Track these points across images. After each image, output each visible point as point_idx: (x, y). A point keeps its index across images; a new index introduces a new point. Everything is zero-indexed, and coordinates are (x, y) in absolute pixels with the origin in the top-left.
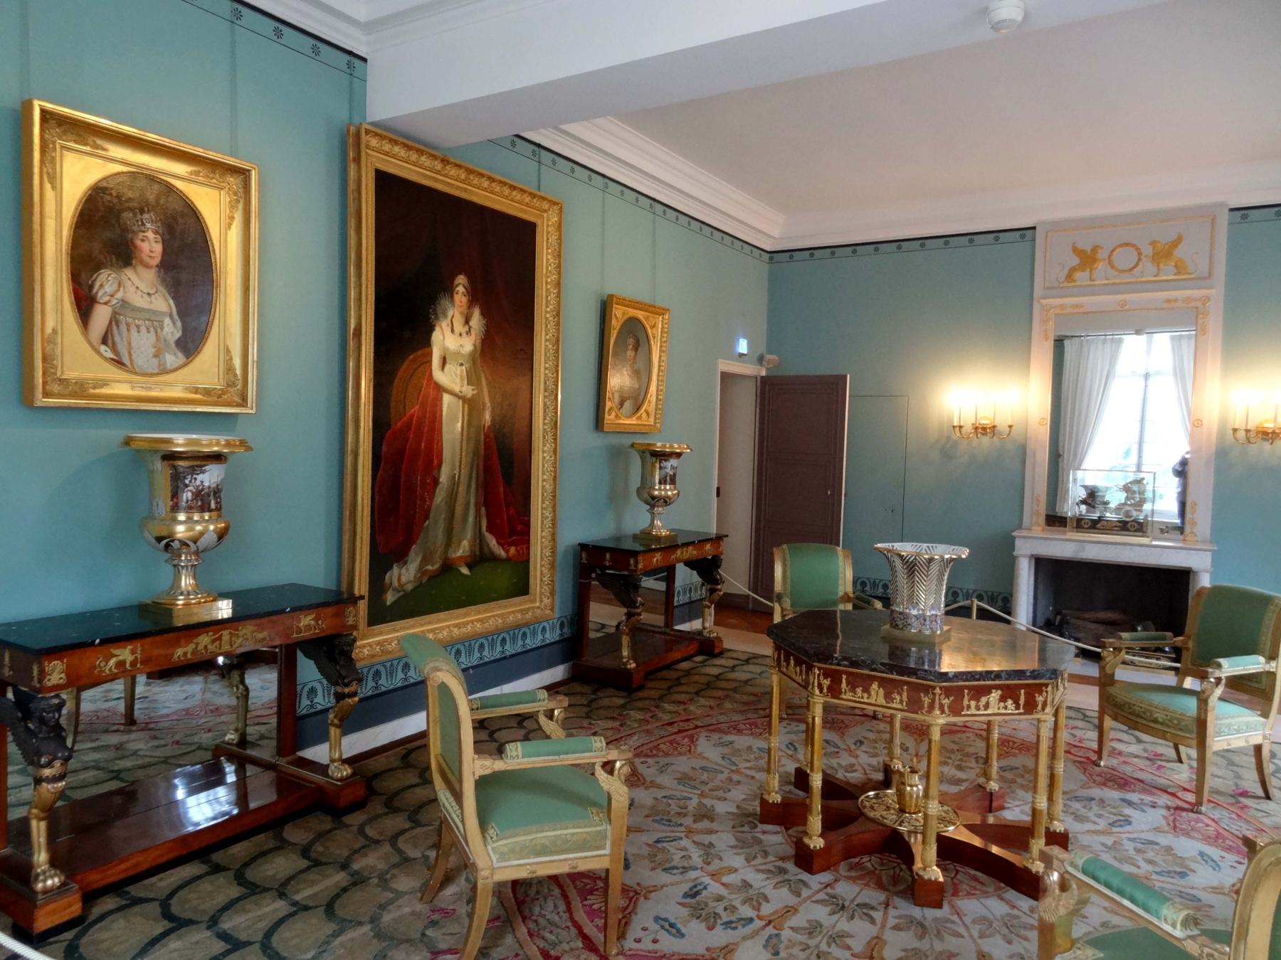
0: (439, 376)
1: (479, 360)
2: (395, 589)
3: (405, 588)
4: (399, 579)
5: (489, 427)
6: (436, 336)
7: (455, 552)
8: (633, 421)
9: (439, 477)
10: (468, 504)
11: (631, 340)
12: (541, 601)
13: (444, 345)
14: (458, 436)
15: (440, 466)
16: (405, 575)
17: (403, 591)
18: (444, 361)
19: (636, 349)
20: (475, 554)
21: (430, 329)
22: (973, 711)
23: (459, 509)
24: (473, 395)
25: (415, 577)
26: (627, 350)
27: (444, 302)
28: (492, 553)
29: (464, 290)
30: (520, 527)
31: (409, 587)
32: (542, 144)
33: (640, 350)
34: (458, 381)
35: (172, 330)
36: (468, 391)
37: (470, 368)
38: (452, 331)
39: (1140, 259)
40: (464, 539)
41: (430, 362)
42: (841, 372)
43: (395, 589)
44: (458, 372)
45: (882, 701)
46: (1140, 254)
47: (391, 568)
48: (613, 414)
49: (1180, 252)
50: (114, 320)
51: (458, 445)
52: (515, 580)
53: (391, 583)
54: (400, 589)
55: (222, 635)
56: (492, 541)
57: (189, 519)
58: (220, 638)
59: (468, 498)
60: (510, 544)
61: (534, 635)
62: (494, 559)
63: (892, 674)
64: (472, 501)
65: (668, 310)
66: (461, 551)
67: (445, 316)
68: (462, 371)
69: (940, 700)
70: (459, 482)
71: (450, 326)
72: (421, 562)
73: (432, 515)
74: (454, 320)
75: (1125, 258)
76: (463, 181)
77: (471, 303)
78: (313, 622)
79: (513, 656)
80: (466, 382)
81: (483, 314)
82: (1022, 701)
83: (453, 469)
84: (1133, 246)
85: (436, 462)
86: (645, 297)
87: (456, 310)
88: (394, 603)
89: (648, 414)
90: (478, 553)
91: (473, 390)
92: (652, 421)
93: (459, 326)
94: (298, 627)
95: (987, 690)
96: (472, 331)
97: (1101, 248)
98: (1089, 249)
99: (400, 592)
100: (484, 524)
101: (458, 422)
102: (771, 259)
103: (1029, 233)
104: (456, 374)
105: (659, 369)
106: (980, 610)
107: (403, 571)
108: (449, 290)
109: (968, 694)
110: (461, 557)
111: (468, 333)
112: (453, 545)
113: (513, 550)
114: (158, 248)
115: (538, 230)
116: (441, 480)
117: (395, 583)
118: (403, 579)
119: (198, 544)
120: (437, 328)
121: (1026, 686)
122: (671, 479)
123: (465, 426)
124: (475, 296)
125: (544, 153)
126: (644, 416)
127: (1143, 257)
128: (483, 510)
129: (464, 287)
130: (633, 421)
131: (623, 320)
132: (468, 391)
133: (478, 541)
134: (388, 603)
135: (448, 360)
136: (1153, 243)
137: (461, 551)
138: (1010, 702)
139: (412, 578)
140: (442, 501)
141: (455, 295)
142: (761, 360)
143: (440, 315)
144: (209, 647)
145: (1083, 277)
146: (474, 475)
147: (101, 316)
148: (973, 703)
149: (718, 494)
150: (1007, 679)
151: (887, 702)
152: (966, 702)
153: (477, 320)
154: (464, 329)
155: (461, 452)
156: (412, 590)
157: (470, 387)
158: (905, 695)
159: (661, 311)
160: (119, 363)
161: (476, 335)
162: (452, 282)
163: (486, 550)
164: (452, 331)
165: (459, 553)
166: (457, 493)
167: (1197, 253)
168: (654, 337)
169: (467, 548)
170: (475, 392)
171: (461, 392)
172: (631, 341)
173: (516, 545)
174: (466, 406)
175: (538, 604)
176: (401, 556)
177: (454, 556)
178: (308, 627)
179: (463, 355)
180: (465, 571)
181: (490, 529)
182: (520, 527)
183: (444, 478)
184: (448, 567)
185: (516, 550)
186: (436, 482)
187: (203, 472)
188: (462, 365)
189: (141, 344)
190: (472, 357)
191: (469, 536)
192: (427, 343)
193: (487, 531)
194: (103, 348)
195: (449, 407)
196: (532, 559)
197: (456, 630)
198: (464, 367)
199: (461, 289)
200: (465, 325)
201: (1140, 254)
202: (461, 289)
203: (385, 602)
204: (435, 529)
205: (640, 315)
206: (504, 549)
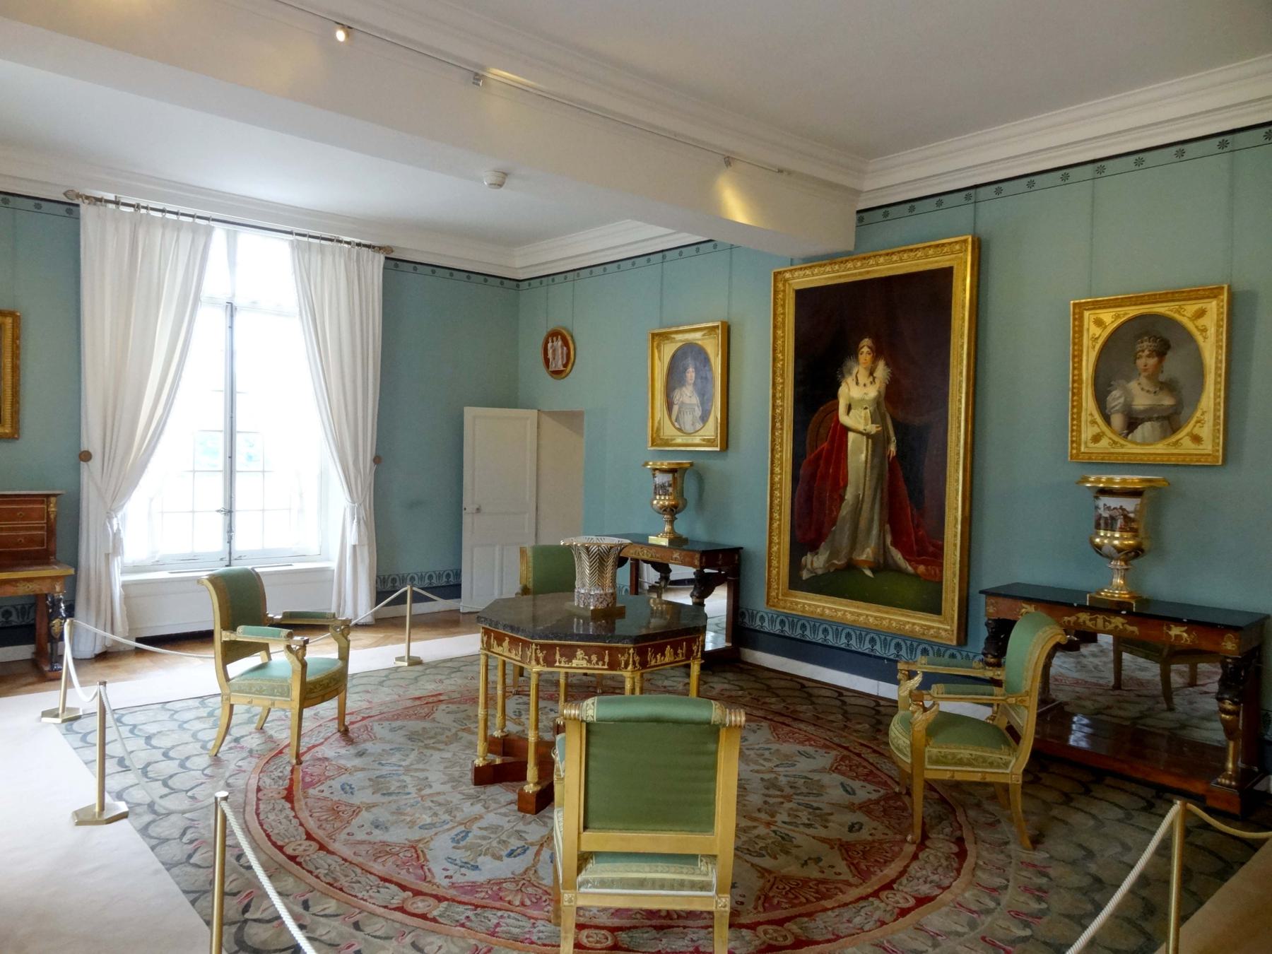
0: (844, 419)
1: (883, 404)
2: (808, 570)
4: (812, 564)
5: (893, 457)
7: (859, 555)
8: (1160, 448)
10: (871, 520)
11: (1145, 344)
13: (849, 394)
15: (845, 486)
16: (817, 562)
18: (849, 408)
20: (879, 562)
21: (838, 385)
23: (863, 523)
24: (877, 431)
26: (1136, 358)
27: (850, 363)
28: (895, 563)
30: (931, 549)
31: (820, 572)
32: (978, 183)
33: (1170, 354)
34: (862, 421)
35: (698, 412)
37: (875, 410)
38: (857, 383)
40: (868, 547)
41: (837, 409)
43: (808, 570)
44: (863, 414)
48: (1104, 443)
50: (679, 412)
51: (862, 470)
52: (925, 596)
53: (806, 565)
56: (898, 556)
57: (660, 499)
59: (872, 516)
62: (899, 571)
64: (876, 517)
67: (850, 373)
68: (865, 414)
72: (829, 556)
73: (838, 523)
76: (862, 267)
77: (875, 360)
80: (870, 422)
81: (887, 364)
83: (857, 488)
85: (842, 484)
88: (807, 580)
90: (882, 561)
96: (876, 380)
100: (889, 540)
101: (862, 453)
104: (861, 417)
105: (1216, 374)
107: (815, 559)
108: (854, 353)
110: (864, 561)
111: (873, 382)
113: (922, 568)
114: (694, 375)
116: (846, 497)
117: (809, 566)
118: (815, 565)
122: (1106, 524)
123: (869, 457)
124: (877, 353)
128: (887, 527)
129: (869, 347)
130: (1160, 448)
131: (1115, 325)
132: (873, 429)
133: (882, 552)
134: (804, 578)
139: (822, 566)
143: (846, 376)
146: (878, 497)
147: (676, 408)
153: (882, 371)
154: (868, 381)
155: (865, 476)
156: (823, 574)
157: (874, 426)
160: (680, 430)
162: (858, 347)
163: (891, 561)
164: (857, 383)
165: (864, 557)
166: (861, 508)
169: (871, 555)
170: (880, 429)
172: (1146, 345)
174: (870, 441)
175: (949, 628)
176: (814, 548)
177: (858, 558)
179: (867, 401)
180: (868, 573)
181: (895, 544)
182: (931, 549)
183: (849, 495)
185: (927, 570)
186: (842, 499)
188: (866, 408)
189: (688, 421)
190: (877, 402)
191: (873, 545)
192: (835, 397)
193: (891, 545)
194: (676, 424)
195: (853, 442)
197: (849, 616)
198: (868, 411)
199: (865, 350)
200: (869, 376)
202: (865, 350)
203: (801, 577)
204: (842, 534)
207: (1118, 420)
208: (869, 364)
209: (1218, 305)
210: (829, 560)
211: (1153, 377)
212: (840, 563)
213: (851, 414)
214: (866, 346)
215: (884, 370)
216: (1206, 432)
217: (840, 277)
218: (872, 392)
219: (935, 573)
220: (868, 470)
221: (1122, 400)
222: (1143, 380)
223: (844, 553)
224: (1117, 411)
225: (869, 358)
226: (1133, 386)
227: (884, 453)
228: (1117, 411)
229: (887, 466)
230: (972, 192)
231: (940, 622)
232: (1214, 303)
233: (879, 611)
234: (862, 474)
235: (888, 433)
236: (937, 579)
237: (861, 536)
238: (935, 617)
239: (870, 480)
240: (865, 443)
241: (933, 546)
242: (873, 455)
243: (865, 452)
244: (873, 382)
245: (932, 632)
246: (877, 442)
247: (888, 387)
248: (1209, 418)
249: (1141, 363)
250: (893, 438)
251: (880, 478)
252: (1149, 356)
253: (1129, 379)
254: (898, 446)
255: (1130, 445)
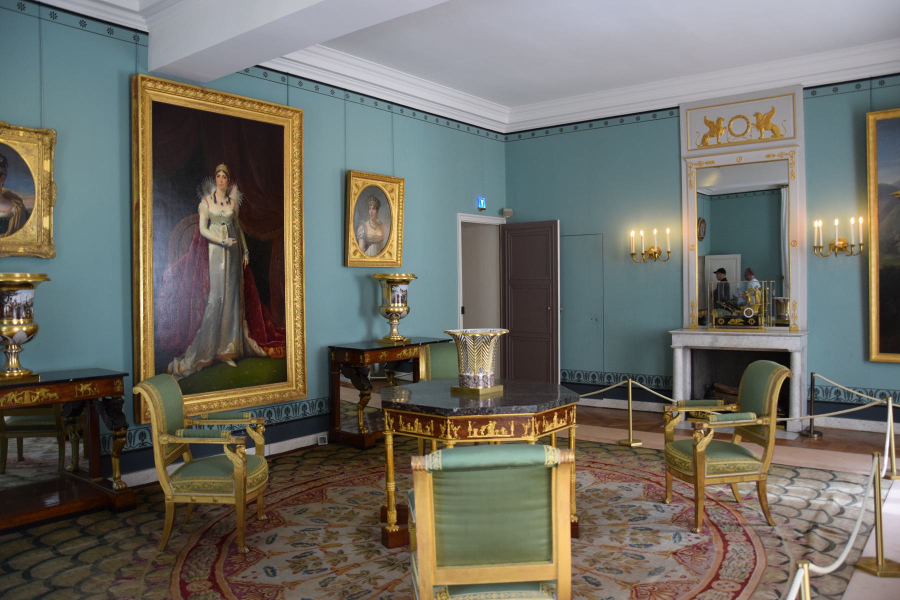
0: (204, 231)
1: (237, 221)
2: (175, 375)
3: (184, 374)
6: (203, 206)
8: (378, 259)
9: (208, 299)
11: (372, 201)
12: (297, 386)
13: (208, 211)
14: (223, 273)
17: (183, 376)
18: (209, 223)
19: (377, 208)
20: (240, 352)
21: (199, 201)
22: (475, 435)
23: (225, 322)
25: (191, 367)
27: (209, 183)
29: (224, 174)
30: (277, 334)
31: (187, 374)
32: (290, 72)
33: (380, 208)
34: (221, 235)
36: (230, 242)
37: (231, 226)
38: (215, 202)
39: (748, 127)
40: (230, 342)
41: (198, 223)
42: (555, 219)
44: (221, 229)
45: (421, 431)
46: (748, 123)
47: (173, 360)
48: (358, 255)
49: (772, 121)
52: (274, 371)
53: (173, 371)
54: (179, 374)
55: (24, 393)
56: (254, 344)
58: (23, 395)
60: (269, 346)
61: (296, 411)
62: (256, 356)
63: (423, 412)
65: (403, 180)
66: (228, 350)
67: (209, 192)
68: (224, 229)
69: (450, 428)
70: (224, 304)
71: (213, 198)
72: (196, 357)
74: (216, 194)
75: (738, 127)
76: (221, 103)
77: (230, 183)
78: (89, 389)
79: (277, 424)
80: (227, 236)
81: (239, 189)
82: (512, 429)
83: (219, 294)
84: (743, 117)
86: (385, 171)
87: (218, 188)
89: (390, 254)
90: (242, 352)
91: (233, 241)
92: (395, 259)
93: (220, 197)
94: (78, 391)
95: (486, 421)
96: (231, 201)
97: (723, 120)
98: (715, 121)
99: (180, 376)
100: (247, 333)
101: (222, 262)
102: (506, 139)
103: (675, 111)
104: (219, 231)
105: (398, 222)
106: (635, 388)
107: (182, 362)
108: (213, 175)
109: (471, 424)
110: (228, 355)
111: (229, 202)
112: (221, 346)
113: (271, 350)
115: (286, 130)
116: (209, 302)
117: (176, 371)
118: (182, 368)
119: (14, 338)
120: (203, 201)
121: (516, 418)
124: (232, 178)
125: (291, 78)
126: (387, 255)
127: (750, 125)
128: (245, 322)
129: (224, 172)
130: (378, 259)
131: (363, 188)
132: (230, 242)
133: (242, 343)
135: (212, 221)
136: (756, 115)
137: (228, 350)
138: (503, 429)
139: (189, 368)
140: (210, 316)
141: (217, 178)
142: (502, 213)
144: (16, 400)
145: (710, 141)
148: (476, 431)
149: (463, 312)
150: (497, 413)
151: (424, 432)
152: (470, 429)
153: (235, 193)
154: (225, 201)
155: (225, 282)
156: (190, 376)
158: (432, 425)
159: (398, 181)
161: (235, 204)
162: (215, 170)
163: (249, 350)
164: (215, 202)
165: (227, 351)
167: (785, 121)
168: (393, 199)
169: (233, 349)
170: (235, 242)
171: (223, 242)
172: (372, 204)
173: (274, 347)
174: (228, 252)
175: (294, 388)
177: (222, 353)
178: (86, 392)
180: (232, 364)
181: (252, 335)
182: (277, 334)
184: (217, 362)
185: (275, 351)
187: (16, 294)
188: (223, 224)
190: (232, 219)
191: (234, 340)
192: (196, 211)
193: (249, 337)
196: (288, 357)
198: (225, 226)
199: (221, 174)
200: (225, 197)
201: (748, 123)
202: (221, 174)
205: (379, 184)
206: (263, 350)
207: (361, 242)
208: (225, 186)
209: (399, 187)
210: (196, 361)
211: (374, 220)
212: (206, 361)
213: (211, 227)
214: (222, 171)
215: (237, 193)
216: (394, 250)
217: (200, 104)
218: (228, 211)
219: (281, 352)
220: (228, 277)
221: (363, 232)
222: (371, 221)
223: (210, 351)
224: (361, 238)
225: (224, 181)
226: (367, 223)
227: (240, 262)
228: (361, 238)
229: (242, 273)
230: (285, 76)
231: (289, 386)
232: (397, 185)
233: (245, 392)
234: (222, 280)
235: (242, 245)
236: (282, 356)
237: (224, 333)
238: (284, 384)
239: (229, 285)
240: (224, 254)
241: (278, 332)
242: (231, 264)
243: (224, 261)
244: (229, 202)
245: (287, 395)
246: (234, 252)
247: (240, 208)
248: (395, 244)
249: (370, 211)
250: (246, 250)
251: (238, 281)
252: (373, 208)
253: (366, 221)
254: (250, 256)
255: (367, 257)
